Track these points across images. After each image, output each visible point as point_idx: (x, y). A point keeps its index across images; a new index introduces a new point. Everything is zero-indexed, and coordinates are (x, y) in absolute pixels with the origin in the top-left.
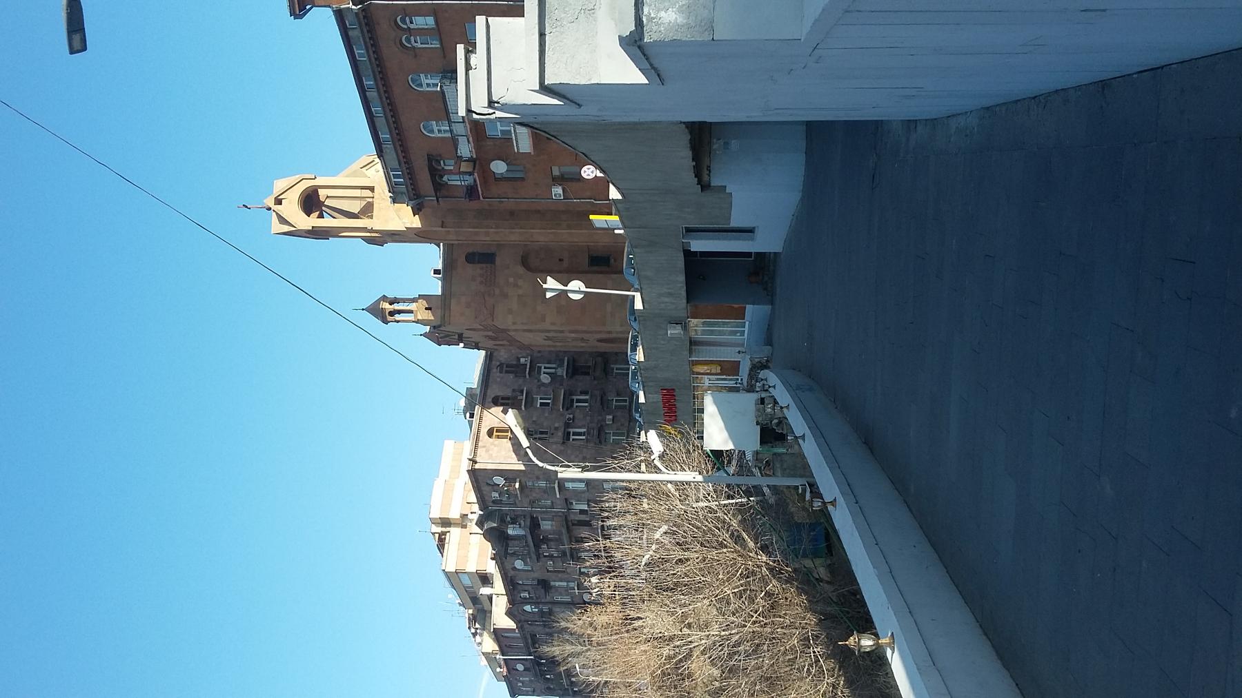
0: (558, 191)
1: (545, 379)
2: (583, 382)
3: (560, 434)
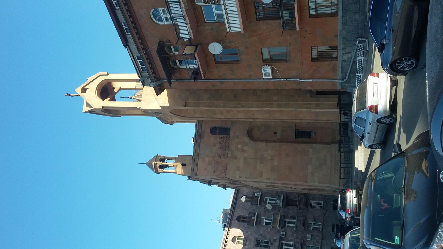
0: (267, 70)
1: (269, 207)
2: (292, 210)
3: (277, 244)
